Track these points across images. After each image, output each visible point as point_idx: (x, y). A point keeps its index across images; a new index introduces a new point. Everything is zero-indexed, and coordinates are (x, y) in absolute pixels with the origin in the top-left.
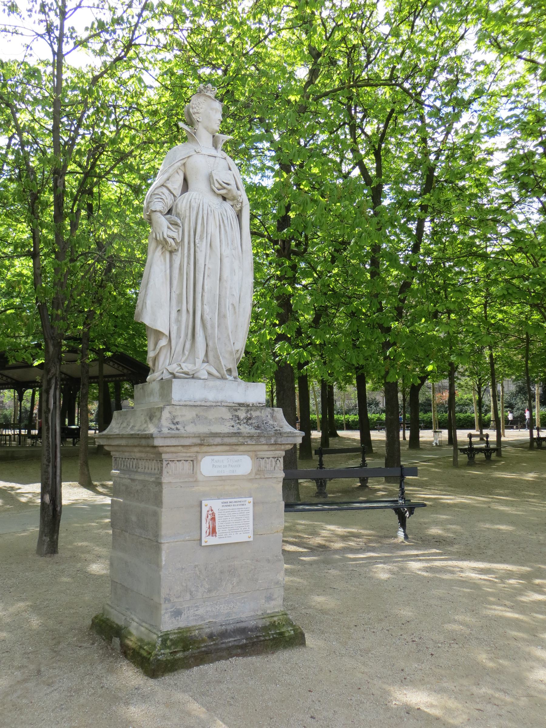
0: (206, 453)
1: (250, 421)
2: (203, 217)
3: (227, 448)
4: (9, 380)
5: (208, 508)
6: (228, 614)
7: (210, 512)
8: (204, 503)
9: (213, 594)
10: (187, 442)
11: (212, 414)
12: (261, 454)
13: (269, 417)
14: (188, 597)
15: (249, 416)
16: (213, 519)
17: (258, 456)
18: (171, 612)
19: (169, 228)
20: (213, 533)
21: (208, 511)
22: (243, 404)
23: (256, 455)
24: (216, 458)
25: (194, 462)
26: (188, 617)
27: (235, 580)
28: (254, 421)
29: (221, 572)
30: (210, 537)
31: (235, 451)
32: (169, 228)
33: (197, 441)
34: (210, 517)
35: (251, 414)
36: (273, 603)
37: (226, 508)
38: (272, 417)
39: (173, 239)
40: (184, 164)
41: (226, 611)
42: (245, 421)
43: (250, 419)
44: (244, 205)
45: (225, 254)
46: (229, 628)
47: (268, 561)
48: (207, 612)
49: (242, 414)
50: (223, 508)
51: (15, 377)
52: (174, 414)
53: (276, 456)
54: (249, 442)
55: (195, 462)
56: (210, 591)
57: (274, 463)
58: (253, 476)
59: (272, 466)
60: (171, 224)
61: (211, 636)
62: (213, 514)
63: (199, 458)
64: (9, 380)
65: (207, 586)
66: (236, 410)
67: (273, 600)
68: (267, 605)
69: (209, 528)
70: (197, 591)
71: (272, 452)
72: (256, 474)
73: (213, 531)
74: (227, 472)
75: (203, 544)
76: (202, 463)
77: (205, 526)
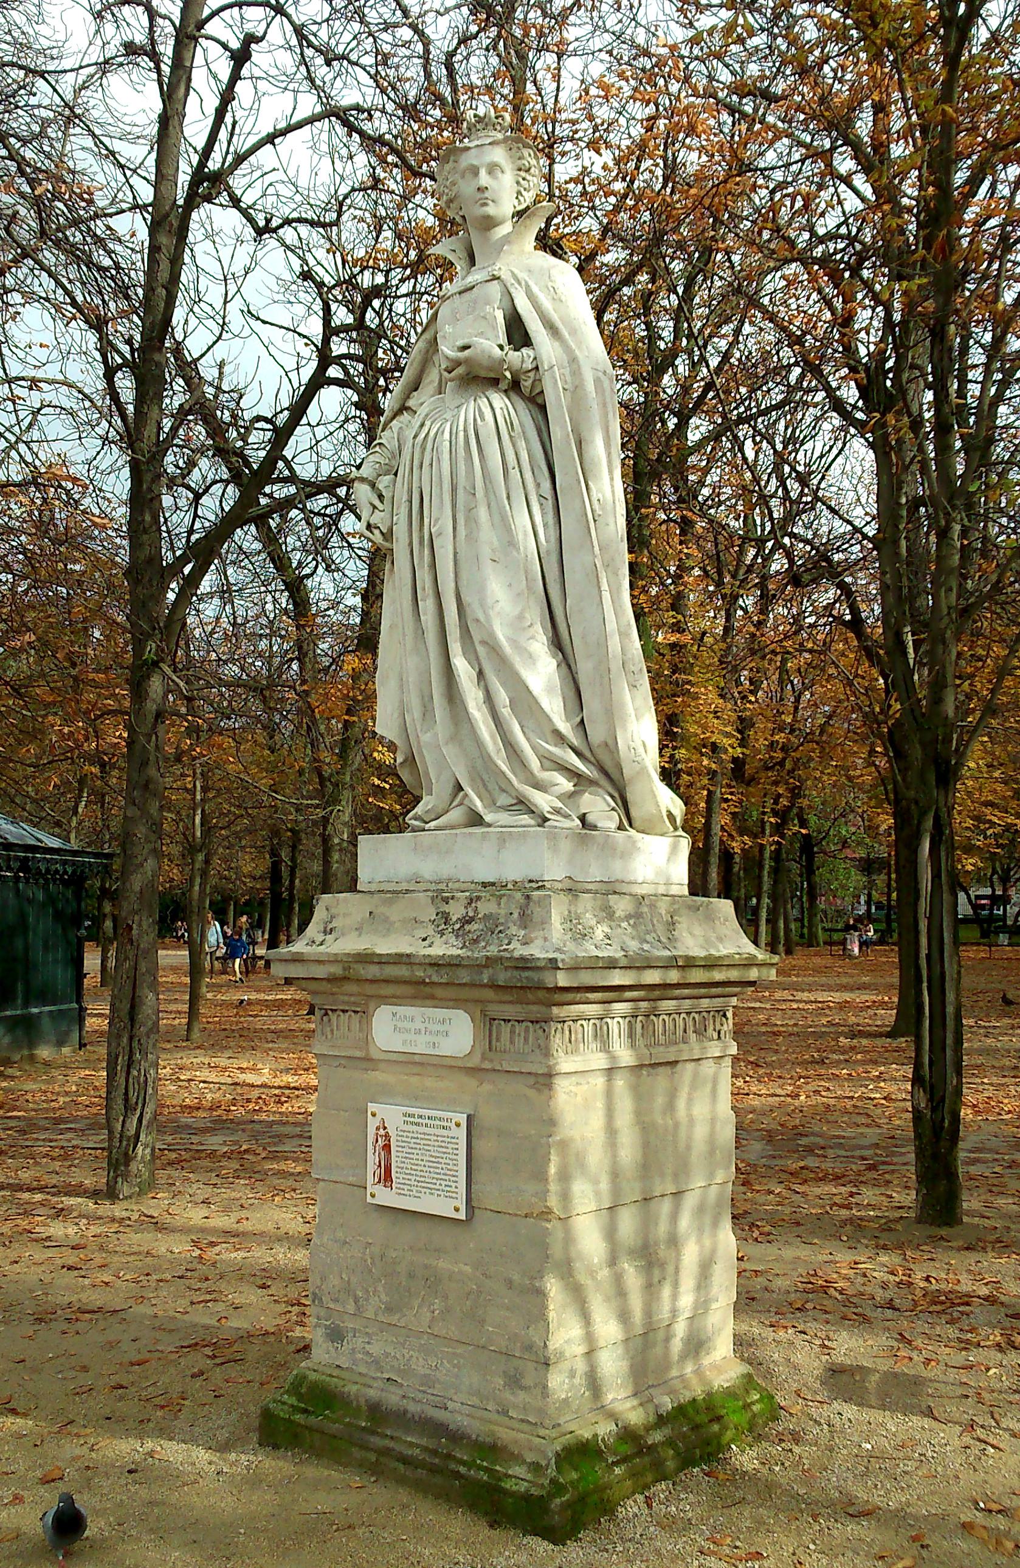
1: (467, 927)
3: (408, 990)
6: (428, 1381)
7: (382, 1132)
8: (372, 1107)
9: (394, 1319)
10: (320, 972)
11: (396, 912)
12: (495, 1010)
13: (516, 915)
14: (351, 1308)
15: (471, 914)
16: (387, 1147)
18: (326, 1327)
22: (493, 884)
23: (483, 1012)
24: (401, 1010)
25: (365, 1014)
26: (353, 1349)
27: (438, 1304)
28: (476, 926)
29: (411, 1276)
30: (381, 1186)
31: (432, 997)
33: (336, 970)
35: (476, 909)
36: (522, 1396)
38: (522, 915)
41: (422, 1371)
42: (457, 926)
43: (470, 921)
46: (412, 1408)
47: (510, 1284)
48: (387, 1355)
49: (457, 911)
52: (333, 911)
54: (435, 979)
56: (389, 1309)
61: (375, 1410)
62: (387, 1136)
63: (371, 1009)
65: (383, 1297)
66: (446, 901)
67: (522, 1388)
68: (507, 1395)
70: (367, 1300)
72: (484, 1058)
73: (387, 1177)
74: (421, 1046)
75: (369, 1199)
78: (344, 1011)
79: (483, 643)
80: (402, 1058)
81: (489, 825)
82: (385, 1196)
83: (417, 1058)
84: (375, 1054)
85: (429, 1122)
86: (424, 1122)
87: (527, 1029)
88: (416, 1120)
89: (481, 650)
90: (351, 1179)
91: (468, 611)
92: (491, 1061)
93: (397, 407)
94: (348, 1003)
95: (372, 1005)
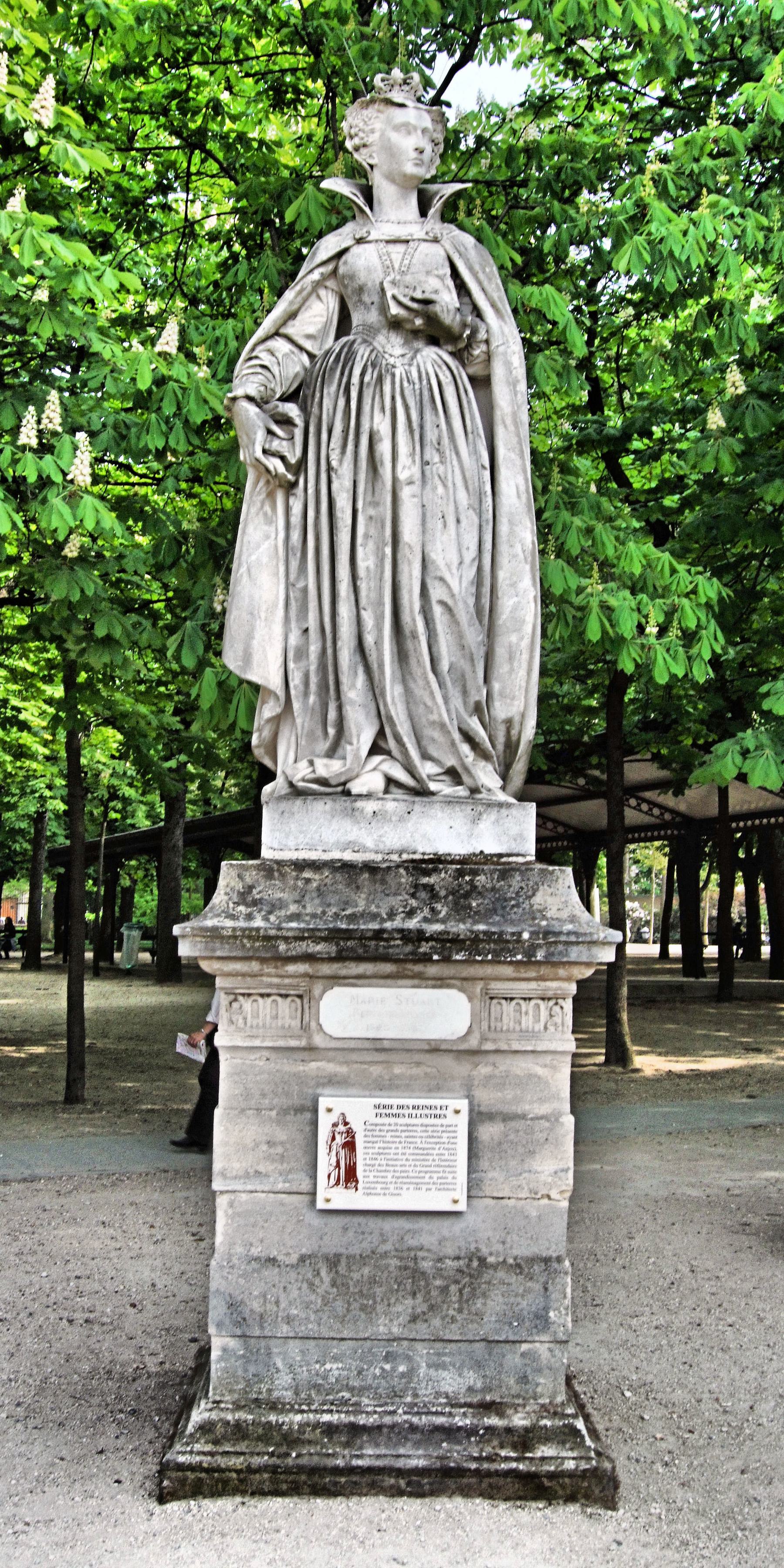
0: (336, 980)
2: (431, 389)
4: (560, 829)
5: (334, 1117)
7: (341, 1128)
8: (324, 1103)
16: (350, 1146)
17: (492, 993)
19: (270, 432)
20: (347, 1181)
21: (335, 1125)
30: (340, 1189)
31: (419, 976)
32: (270, 432)
34: (340, 1140)
37: (386, 1120)
39: (283, 458)
40: (335, 271)
44: (493, 345)
45: (402, 475)
50: (379, 1120)
51: (574, 821)
53: (550, 994)
55: (306, 1000)
57: (544, 1013)
58: (473, 1043)
59: (537, 1020)
60: (277, 422)
62: (350, 1133)
64: (560, 829)
69: (338, 1165)
71: (533, 985)
72: (484, 1039)
73: (350, 1176)
75: (320, 1205)
76: (322, 1003)
77: (325, 1163)
78: (262, 995)
79: (442, 603)
80: (367, 1045)
81: (433, 794)
82: (343, 1198)
83: (386, 1045)
84: (318, 1040)
85: (414, 1112)
86: (406, 1112)
87: (538, 1006)
88: (395, 1111)
89: (437, 610)
90: (280, 1186)
91: (430, 568)
92: (494, 1041)
93: (273, 331)
94: (270, 985)
95: (317, 989)
